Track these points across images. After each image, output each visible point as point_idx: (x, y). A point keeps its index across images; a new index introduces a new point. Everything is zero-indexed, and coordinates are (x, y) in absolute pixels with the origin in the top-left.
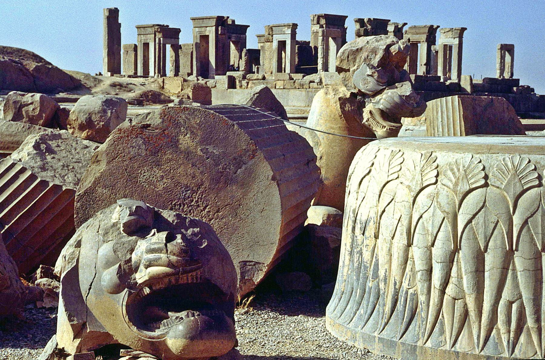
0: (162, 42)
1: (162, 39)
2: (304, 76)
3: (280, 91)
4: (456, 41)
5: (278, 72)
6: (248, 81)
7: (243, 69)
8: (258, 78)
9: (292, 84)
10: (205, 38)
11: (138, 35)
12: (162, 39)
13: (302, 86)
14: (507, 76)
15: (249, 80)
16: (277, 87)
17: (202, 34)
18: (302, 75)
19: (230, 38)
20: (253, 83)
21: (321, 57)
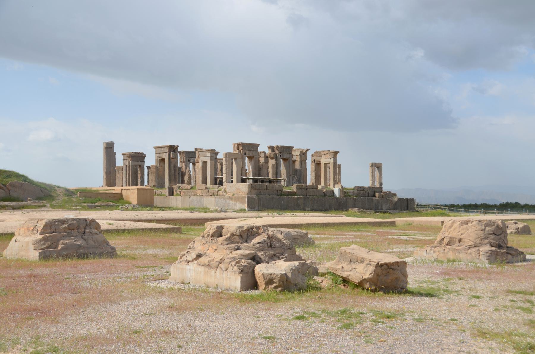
0: (131, 164)
1: (131, 162)
2: (219, 187)
3: (198, 197)
4: (332, 161)
5: (203, 184)
6: (180, 190)
7: (186, 182)
8: (188, 188)
9: (207, 192)
10: (162, 160)
11: (123, 160)
12: (131, 162)
13: (213, 194)
14: (377, 185)
15: (182, 189)
16: (198, 195)
17: (161, 158)
18: (217, 185)
19: (189, 161)
20: (184, 192)
21: (225, 172)
